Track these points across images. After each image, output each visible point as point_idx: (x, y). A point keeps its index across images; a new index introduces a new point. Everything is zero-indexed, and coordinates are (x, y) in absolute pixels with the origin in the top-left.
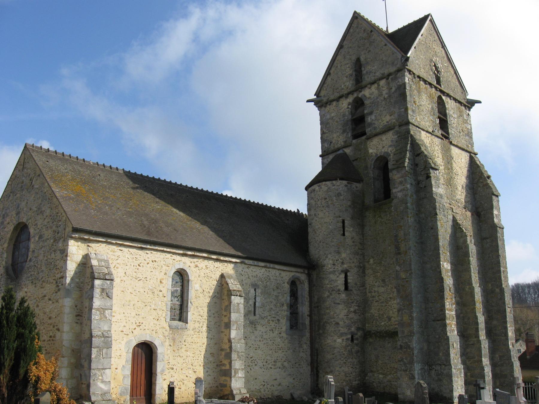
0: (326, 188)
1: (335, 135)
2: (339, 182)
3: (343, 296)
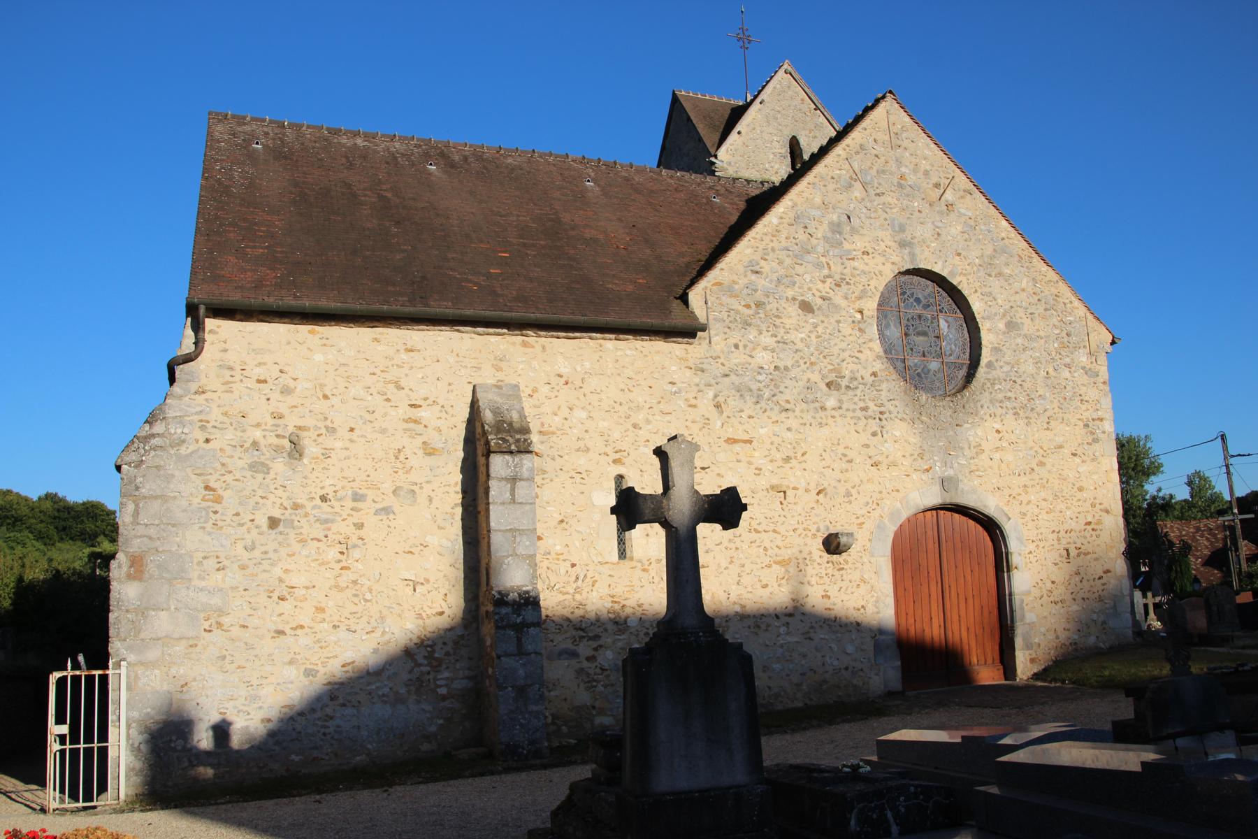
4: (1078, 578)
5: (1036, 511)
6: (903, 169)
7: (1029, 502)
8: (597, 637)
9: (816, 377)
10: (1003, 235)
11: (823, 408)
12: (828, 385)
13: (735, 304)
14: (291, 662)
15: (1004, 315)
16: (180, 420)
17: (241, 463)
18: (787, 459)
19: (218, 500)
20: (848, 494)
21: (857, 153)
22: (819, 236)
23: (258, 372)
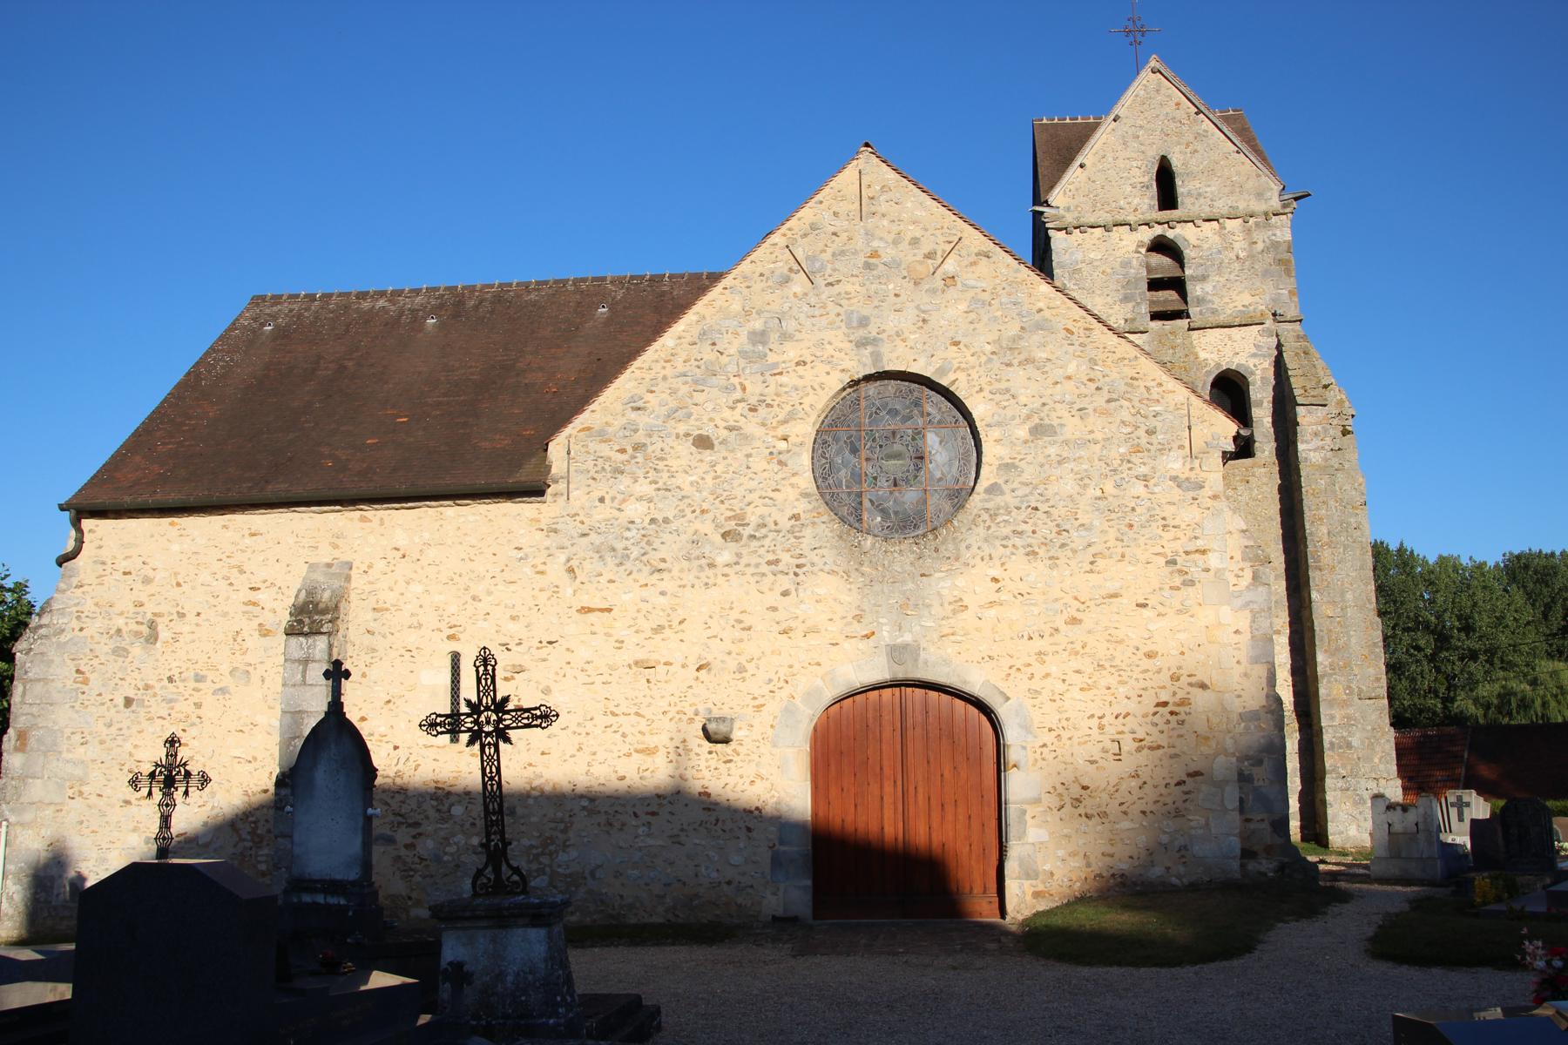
4: (1134, 783)
5: (1060, 687)
6: (875, 244)
7: (1047, 675)
8: (417, 824)
9: (706, 526)
10: (1041, 305)
11: (711, 565)
12: (724, 535)
13: (605, 450)
14: (135, 830)
15: (1028, 417)
16: (62, 612)
17: (106, 649)
18: (659, 629)
19: (86, 682)
20: (741, 669)
21: (805, 235)
22: (732, 351)
23: (124, 565)
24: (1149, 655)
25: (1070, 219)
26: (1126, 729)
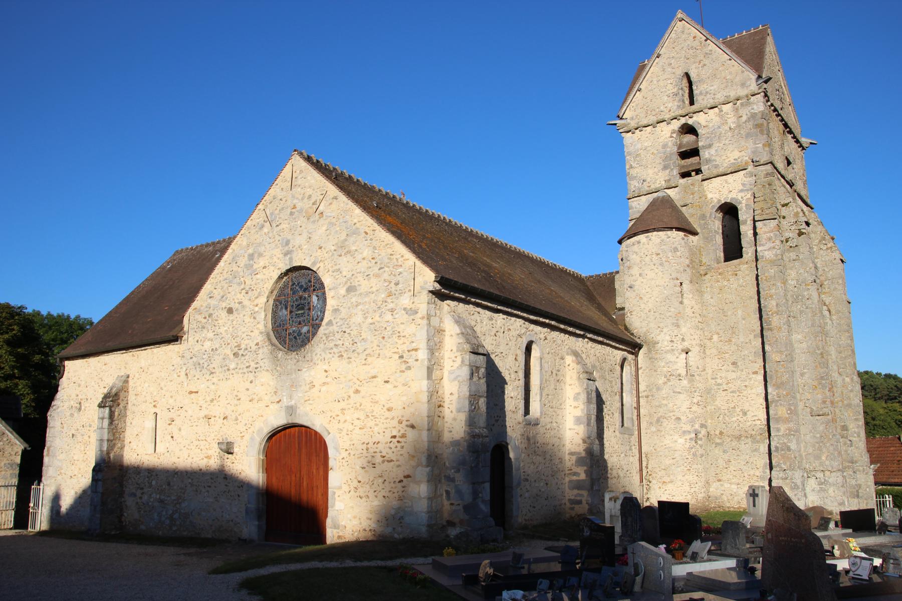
0: (659, 241)
1: (650, 171)
2: (674, 233)
3: (685, 382)
4: (381, 480)
5: (351, 427)
7: (345, 421)
8: (142, 489)
10: (355, 221)
11: (228, 370)
15: (346, 283)
18: (212, 401)
20: (237, 419)
24: (389, 410)
25: (633, 124)
26: (378, 450)
